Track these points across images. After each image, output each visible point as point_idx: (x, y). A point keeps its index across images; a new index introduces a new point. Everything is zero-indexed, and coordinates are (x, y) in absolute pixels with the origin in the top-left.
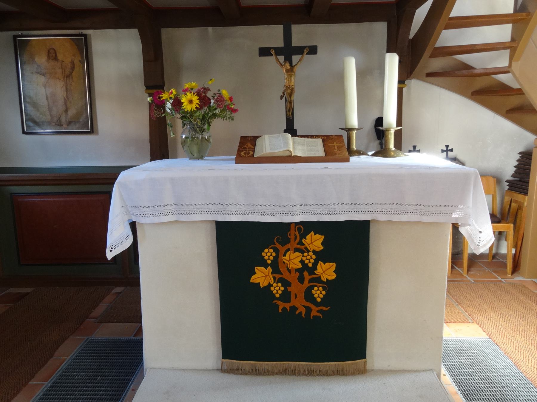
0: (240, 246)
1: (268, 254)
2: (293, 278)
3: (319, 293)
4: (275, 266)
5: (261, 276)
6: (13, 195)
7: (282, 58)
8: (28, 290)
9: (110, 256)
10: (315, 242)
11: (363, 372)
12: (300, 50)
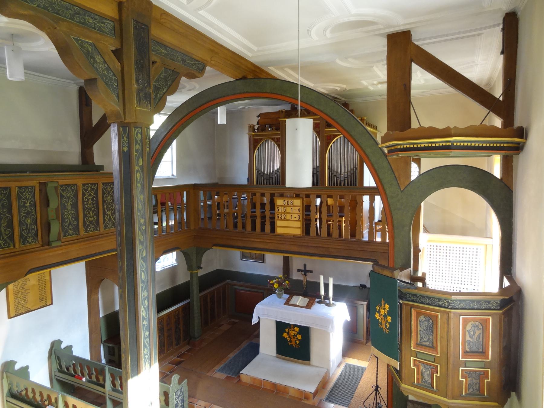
0: (281, 327)
1: (287, 330)
2: (292, 337)
3: (298, 342)
4: (288, 333)
5: (285, 335)
7: (303, 273)
9: (253, 324)
10: (297, 329)
11: (309, 365)
12: (308, 271)
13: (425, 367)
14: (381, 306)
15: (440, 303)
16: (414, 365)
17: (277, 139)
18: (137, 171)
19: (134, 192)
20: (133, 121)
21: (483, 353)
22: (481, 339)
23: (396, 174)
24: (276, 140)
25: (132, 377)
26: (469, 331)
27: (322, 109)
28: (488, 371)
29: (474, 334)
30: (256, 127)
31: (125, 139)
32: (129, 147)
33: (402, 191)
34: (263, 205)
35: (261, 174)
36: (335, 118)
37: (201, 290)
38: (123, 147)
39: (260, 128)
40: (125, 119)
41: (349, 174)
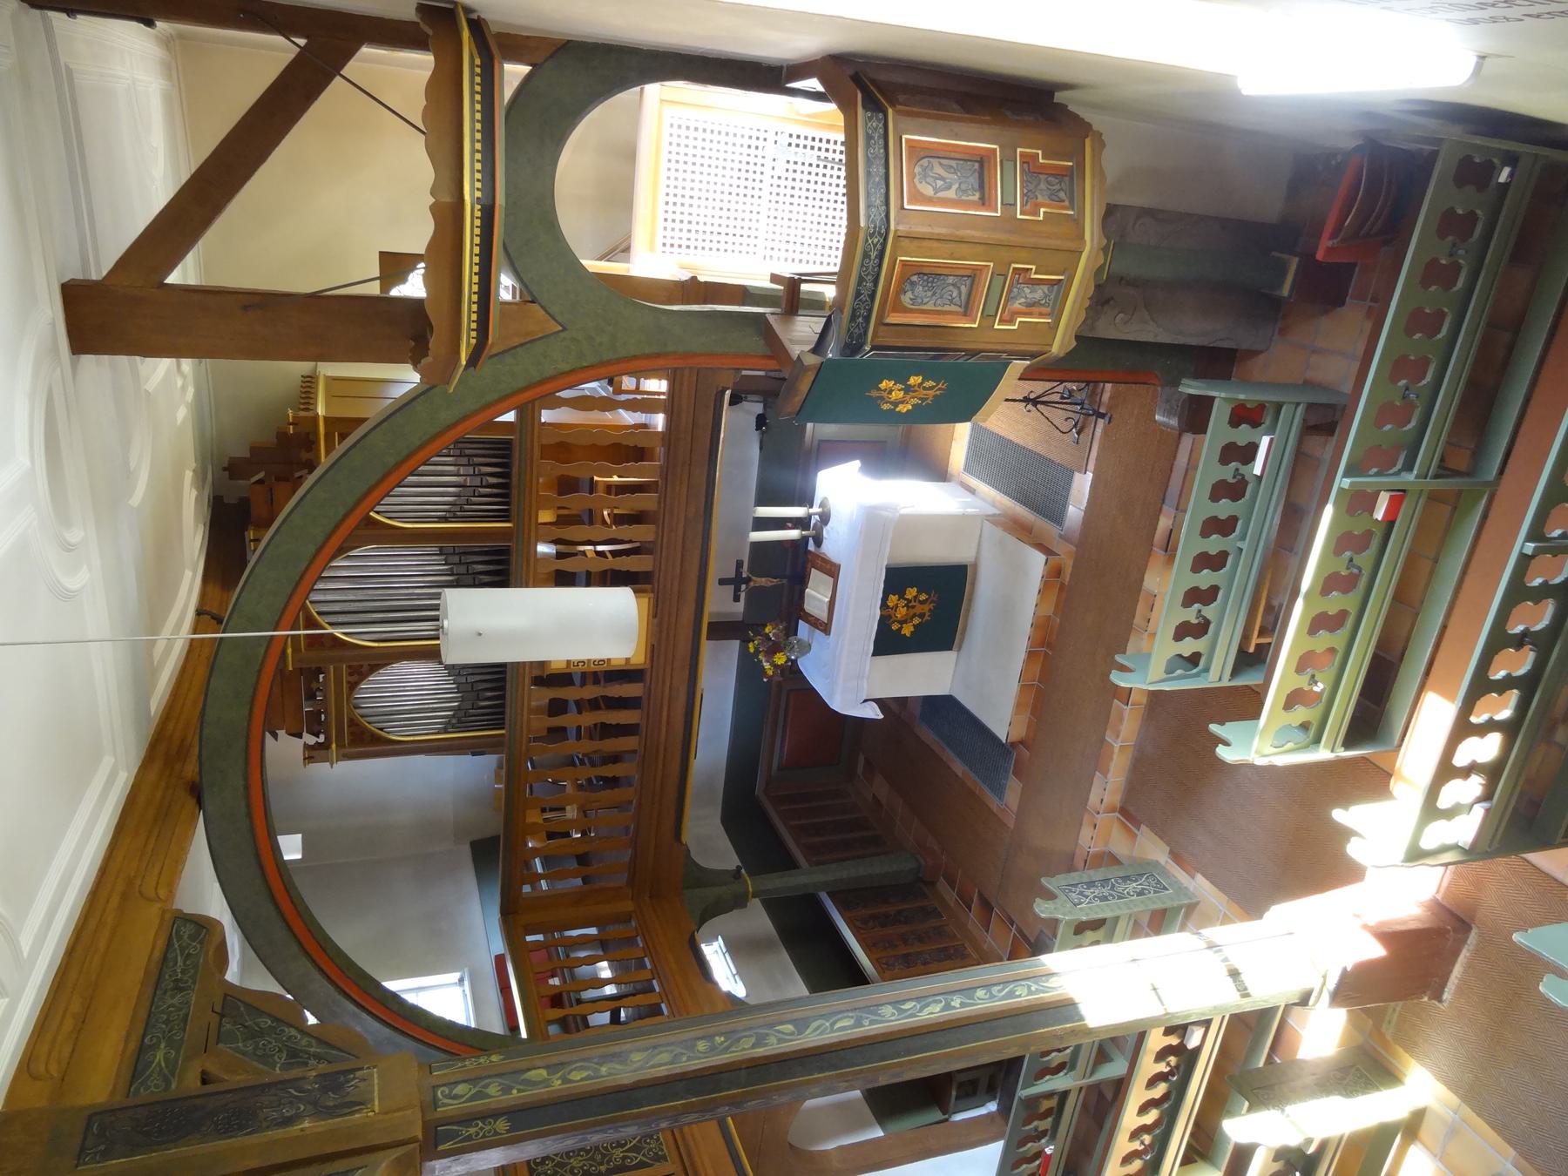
0: (888, 642)
1: (895, 627)
2: (912, 611)
3: (923, 597)
4: (902, 622)
5: (907, 630)
6: (779, 769)
8: (862, 759)
9: (881, 716)
10: (893, 599)
11: (975, 566)
13: (1015, 298)
14: (882, 398)
15: (873, 254)
16: (1011, 321)
17: (351, 674)
18: (565, 1080)
19: (626, 1082)
20: (420, 1115)
21: (982, 162)
22: (953, 163)
23: (517, 341)
24: (353, 679)
25: (1082, 1019)
26: (936, 190)
27: (312, 549)
28: (1022, 155)
29: (943, 179)
30: (310, 739)
31: (472, 1130)
32: (495, 1114)
33: (565, 329)
34: (558, 707)
35: (460, 720)
36: (342, 511)
37: (790, 864)
38: (496, 1133)
39: (316, 728)
40: (413, 1140)
41: (464, 460)
